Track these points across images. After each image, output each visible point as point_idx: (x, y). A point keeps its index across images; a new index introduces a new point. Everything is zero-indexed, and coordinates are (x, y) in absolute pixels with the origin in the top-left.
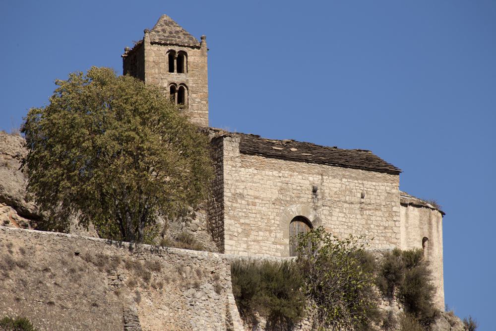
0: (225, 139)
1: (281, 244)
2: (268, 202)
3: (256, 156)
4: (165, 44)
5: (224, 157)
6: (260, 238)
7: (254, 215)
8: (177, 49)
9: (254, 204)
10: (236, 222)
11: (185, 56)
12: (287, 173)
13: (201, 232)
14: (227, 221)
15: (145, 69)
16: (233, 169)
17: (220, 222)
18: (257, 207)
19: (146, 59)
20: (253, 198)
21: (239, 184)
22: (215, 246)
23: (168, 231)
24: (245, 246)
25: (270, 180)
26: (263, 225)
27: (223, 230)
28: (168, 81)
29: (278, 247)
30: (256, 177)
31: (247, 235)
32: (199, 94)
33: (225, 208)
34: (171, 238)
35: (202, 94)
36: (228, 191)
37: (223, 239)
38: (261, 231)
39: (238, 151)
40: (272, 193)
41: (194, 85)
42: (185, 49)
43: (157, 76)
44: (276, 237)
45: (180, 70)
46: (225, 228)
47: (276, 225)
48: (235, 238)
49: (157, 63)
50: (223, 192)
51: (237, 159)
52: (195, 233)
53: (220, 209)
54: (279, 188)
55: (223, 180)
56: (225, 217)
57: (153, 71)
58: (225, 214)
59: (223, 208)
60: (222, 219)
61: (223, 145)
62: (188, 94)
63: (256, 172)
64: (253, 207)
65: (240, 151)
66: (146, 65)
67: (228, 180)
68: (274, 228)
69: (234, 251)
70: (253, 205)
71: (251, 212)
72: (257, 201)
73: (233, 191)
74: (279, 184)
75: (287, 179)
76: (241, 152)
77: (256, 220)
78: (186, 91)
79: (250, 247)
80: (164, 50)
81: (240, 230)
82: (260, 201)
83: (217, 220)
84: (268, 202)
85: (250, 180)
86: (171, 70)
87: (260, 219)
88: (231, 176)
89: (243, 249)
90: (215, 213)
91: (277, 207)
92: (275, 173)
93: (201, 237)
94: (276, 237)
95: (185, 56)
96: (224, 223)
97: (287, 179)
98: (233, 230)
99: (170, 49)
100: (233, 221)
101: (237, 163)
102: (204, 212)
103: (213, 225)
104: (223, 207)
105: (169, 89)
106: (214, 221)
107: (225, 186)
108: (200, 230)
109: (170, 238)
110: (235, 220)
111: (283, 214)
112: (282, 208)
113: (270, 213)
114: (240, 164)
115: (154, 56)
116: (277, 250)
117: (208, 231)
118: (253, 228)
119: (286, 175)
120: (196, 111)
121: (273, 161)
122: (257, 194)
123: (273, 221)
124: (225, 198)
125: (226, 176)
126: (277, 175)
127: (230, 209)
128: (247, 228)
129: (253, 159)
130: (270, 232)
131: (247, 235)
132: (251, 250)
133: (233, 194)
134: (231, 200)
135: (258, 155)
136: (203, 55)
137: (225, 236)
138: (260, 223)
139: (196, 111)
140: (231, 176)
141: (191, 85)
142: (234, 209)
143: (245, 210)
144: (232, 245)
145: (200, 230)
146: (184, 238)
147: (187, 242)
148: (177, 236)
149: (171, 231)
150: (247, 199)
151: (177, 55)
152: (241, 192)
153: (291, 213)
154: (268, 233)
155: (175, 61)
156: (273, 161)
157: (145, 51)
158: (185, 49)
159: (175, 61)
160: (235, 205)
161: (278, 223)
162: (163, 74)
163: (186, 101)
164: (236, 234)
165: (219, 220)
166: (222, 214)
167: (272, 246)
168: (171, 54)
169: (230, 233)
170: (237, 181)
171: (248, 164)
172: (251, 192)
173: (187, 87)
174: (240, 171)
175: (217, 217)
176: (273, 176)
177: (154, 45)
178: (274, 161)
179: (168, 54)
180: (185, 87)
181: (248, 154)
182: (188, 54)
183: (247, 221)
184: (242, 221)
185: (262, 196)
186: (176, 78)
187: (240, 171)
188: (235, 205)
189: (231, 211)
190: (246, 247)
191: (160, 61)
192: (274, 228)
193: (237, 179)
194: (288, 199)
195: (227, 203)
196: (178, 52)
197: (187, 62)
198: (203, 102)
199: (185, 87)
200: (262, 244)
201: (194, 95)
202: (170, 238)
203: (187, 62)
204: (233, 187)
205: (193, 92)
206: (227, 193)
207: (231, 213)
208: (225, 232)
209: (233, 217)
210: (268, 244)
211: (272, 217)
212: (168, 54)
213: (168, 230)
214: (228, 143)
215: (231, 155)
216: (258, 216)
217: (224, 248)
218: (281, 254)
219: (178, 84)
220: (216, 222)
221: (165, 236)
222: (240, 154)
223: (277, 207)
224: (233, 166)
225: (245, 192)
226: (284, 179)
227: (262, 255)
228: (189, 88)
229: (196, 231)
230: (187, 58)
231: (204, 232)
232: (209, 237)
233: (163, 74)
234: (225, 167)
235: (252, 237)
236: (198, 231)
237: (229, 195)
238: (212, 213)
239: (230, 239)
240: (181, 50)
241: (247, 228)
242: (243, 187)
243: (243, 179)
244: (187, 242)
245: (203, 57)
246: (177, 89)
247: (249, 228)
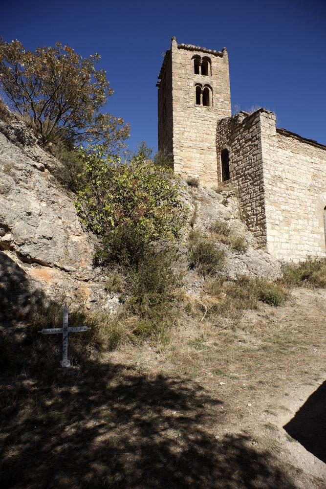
0: (261, 114)
1: (318, 233)
2: (304, 188)
3: (291, 138)
4: (191, 49)
5: (262, 133)
6: (300, 227)
7: (293, 201)
8: (202, 55)
9: (293, 189)
10: (277, 209)
11: (209, 63)
12: (317, 160)
13: (234, 220)
14: (267, 207)
15: (173, 69)
16: (271, 148)
17: (259, 208)
18: (295, 193)
19: (173, 60)
20: (291, 182)
21: (277, 165)
22: (252, 237)
23: (198, 219)
24: (286, 236)
25: (303, 165)
26: (301, 212)
27: (264, 218)
28: (194, 82)
29: (316, 236)
30: (292, 160)
31: (288, 224)
32: (223, 95)
33: (265, 192)
34: (203, 228)
35: (225, 95)
36: (267, 172)
37: (263, 226)
38: (300, 219)
39: (274, 129)
40: (307, 179)
41: (218, 87)
42: (209, 55)
43: (184, 76)
44: (313, 226)
45: (205, 73)
46: (266, 215)
47: (312, 213)
48: (277, 228)
49: (183, 66)
50: (262, 172)
51: (274, 138)
52: (228, 221)
53: (259, 194)
54: (312, 174)
55: (261, 159)
56: (266, 202)
57: (180, 71)
58: (266, 199)
59: (263, 191)
60: (262, 205)
61: (260, 121)
62: (213, 94)
63: (292, 154)
64: (292, 192)
65: (277, 130)
66: (174, 66)
67: (267, 159)
68: (311, 216)
69: (277, 242)
70: (291, 190)
71: (290, 197)
72: (294, 185)
73: (272, 173)
74: (312, 170)
75: (318, 166)
76: (278, 131)
77: (295, 206)
78: (211, 92)
79: (291, 238)
80: (191, 54)
81: (281, 218)
82: (298, 187)
83: (254, 206)
84: (304, 188)
85: (288, 163)
86: (197, 72)
87: (298, 206)
88: (270, 155)
89: (285, 240)
90: (250, 199)
91: (312, 193)
92: (308, 158)
93: (236, 226)
94: (313, 226)
95: (209, 63)
96: (264, 210)
97: (318, 166)
98: (275, 217)
99: (195, 54)
100: (274, 207)
101: (274, 143)
102: (235, 198)
103: (248, 212)
104: (262, 191)
105: (195, 88)
106: (249, 208)
107: (264, 166)
108: (233, 219)
109: (201, 228)
110: (276, 206)
111: (317, 201)
112: (316, 195)
113: (306, 200)
114: (277, 144)
115: (181, 58)
116: (315, 239)
117: (242, 220)
118: (293, 215)
119: (317, 162)
120: (220, 109)
121: (306, 146)
122: (294, 178)
123: (310, 209)
124: (264, 180)
125: (264, 156)
126: (310, 161)
127: (270, 193)
128: (288, 215)
129: (288, 140)
130: (308, 219)
131: (288, 224)
132: (293, 241)
133: (272, 177)
134: (271, 183)
135: (293, 138)
136: (225, 62)
137: (268, 225)
138: (299, 210)
139: (220, 109)
140: (270, 155)
141: (215, 86)
142: (274, 193)
143: (284, 195)
144: (274, 236)
145: (233, 219)
146: (219, 228)
147: (224, 233)
148: (209, 226)
149: (202, 219)
150: (286, 183)
151: (201, 62)
152: (280, 174)
153: (323, 200)
154: (306, 221)
155: (200, 67)
156: (306, 146)
157: (173, 54)
158: (209, 55)
159: (200, 67)
160: (275, 189)
161: (314, 210)
162: (189, 75)
163: (211, 100)
164: (277, 222)
165: (256, 207)
166: (261, 199)
167: (311, 235)
168: (196, 58)
169: (272, 221)
170: (275, 162)
171: (284, 145)
172: (289, 176)
173: (211, 88)
174: (278, 152)
175: (254, 203)
176: (307, 161)
177: (181, 49)
178: (306, 146)
179: (193, 59)
180: (209, 89)
181: (284, 135)
182: (212, 60)
183: (287, 208)
184: (283, 207)
185: (298, 180)
186: (201, 79)
187: (278, 152)
188: (275, 189)
189: (272, 196)
190: (288, 238)
191: (186, 64)
192: (311, 216)
193: (276, 159)
194: (320, 186)
195: (267, 186)
196: (203, 58)
197: (211, 67)
198: (226, 102)
199: (209, 89)
200: (302, 233)
201: (218, 96)
202: (201, 228)
203: (211, 67)
204: (272, 168)
205: (217, 93)
206: (267, 175)
207: (272, 198)
208: (267, 220)
209: (274, 203)
210: (307, 233)
211: (308, 204)
212: (193, 59)
213: (199, 218)
214: (265, 118)
215: (268, 132)
216: (297, 202)
217: (266, 240)
218: (319, 244)
219: (203, 85)
220: (252, 209)
221: (195, 226)
222: (275, 133)
223: (312, 193)
224: (270, 146)
225: (284, 176)
226: (315, 165)
227: (302, 246)
228: (214, 89)
229: (229, 219)
230: (211, 64)
231: (238, 221)
232: (244, 226)
233: (189, 75)
234: (263, 145)
235: (293, 226)
236: (231, 220)
237: (269, 176)
238: (246, 200)
239: (272, 229)
240: (206, 55)
241: (288, 215)
242: (281, 169)
243: (281, 160)
244: (224, 233)
245: (225, 64)
246: (203, 89)
247: (290, 215)
